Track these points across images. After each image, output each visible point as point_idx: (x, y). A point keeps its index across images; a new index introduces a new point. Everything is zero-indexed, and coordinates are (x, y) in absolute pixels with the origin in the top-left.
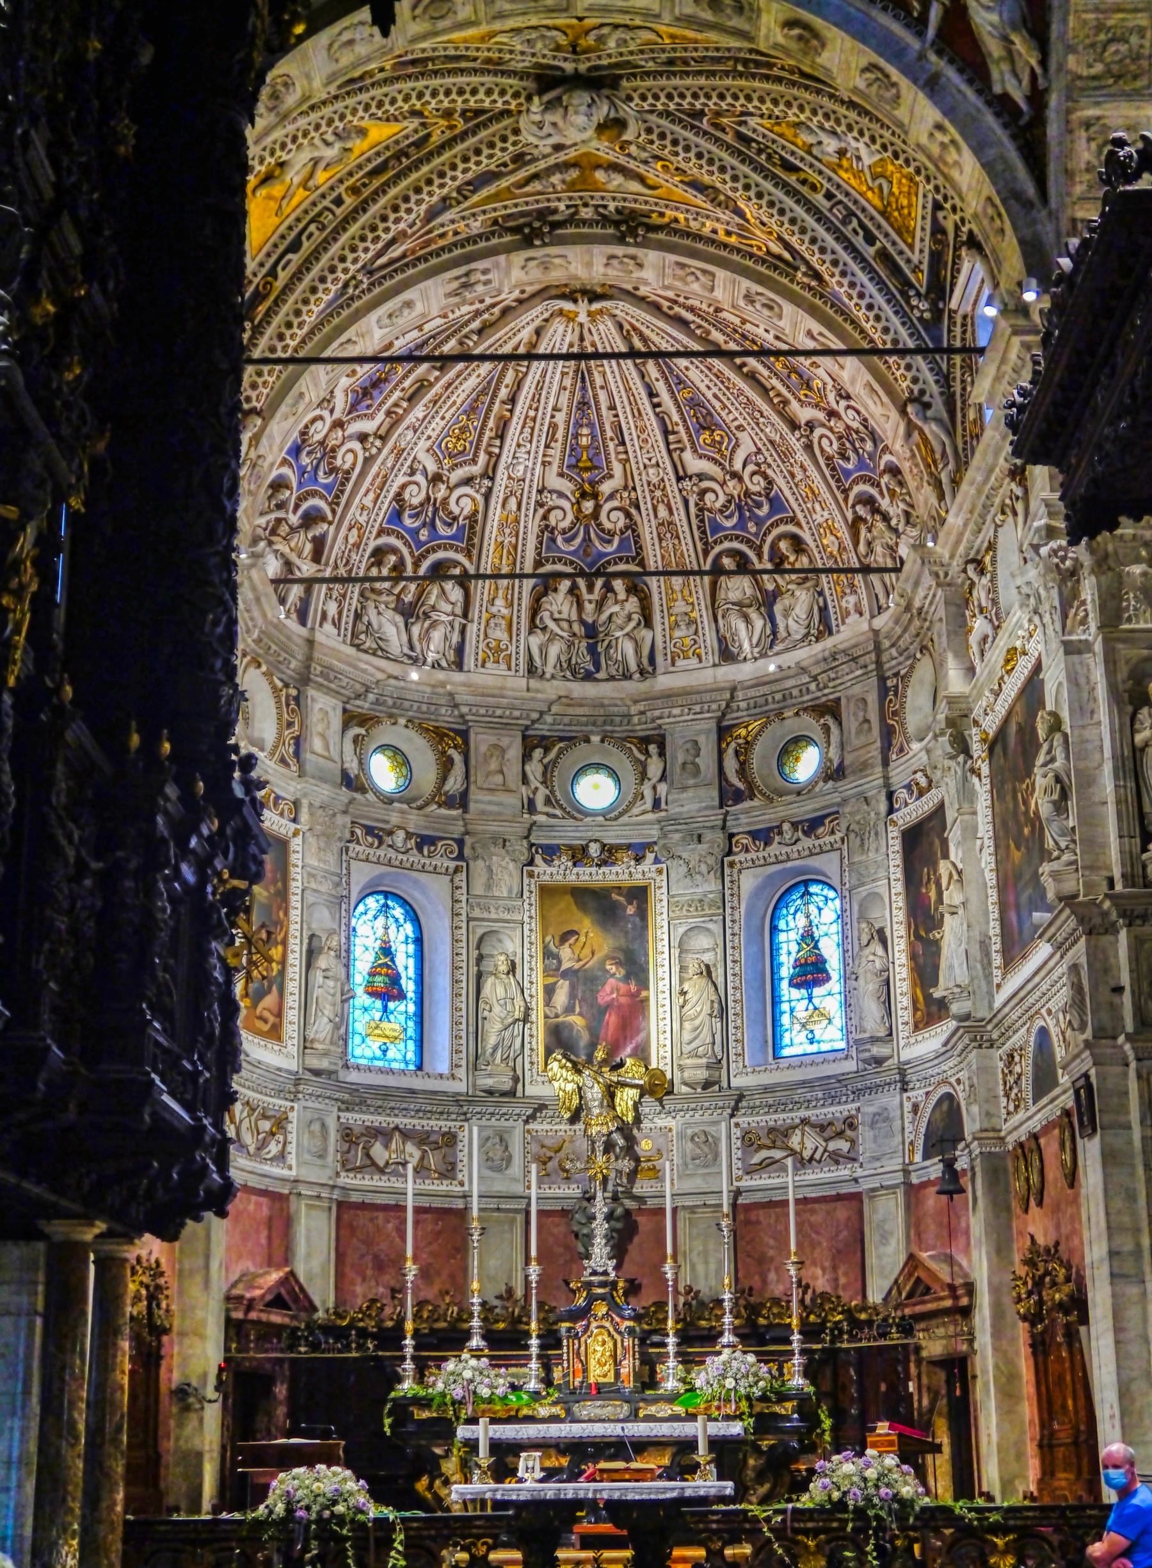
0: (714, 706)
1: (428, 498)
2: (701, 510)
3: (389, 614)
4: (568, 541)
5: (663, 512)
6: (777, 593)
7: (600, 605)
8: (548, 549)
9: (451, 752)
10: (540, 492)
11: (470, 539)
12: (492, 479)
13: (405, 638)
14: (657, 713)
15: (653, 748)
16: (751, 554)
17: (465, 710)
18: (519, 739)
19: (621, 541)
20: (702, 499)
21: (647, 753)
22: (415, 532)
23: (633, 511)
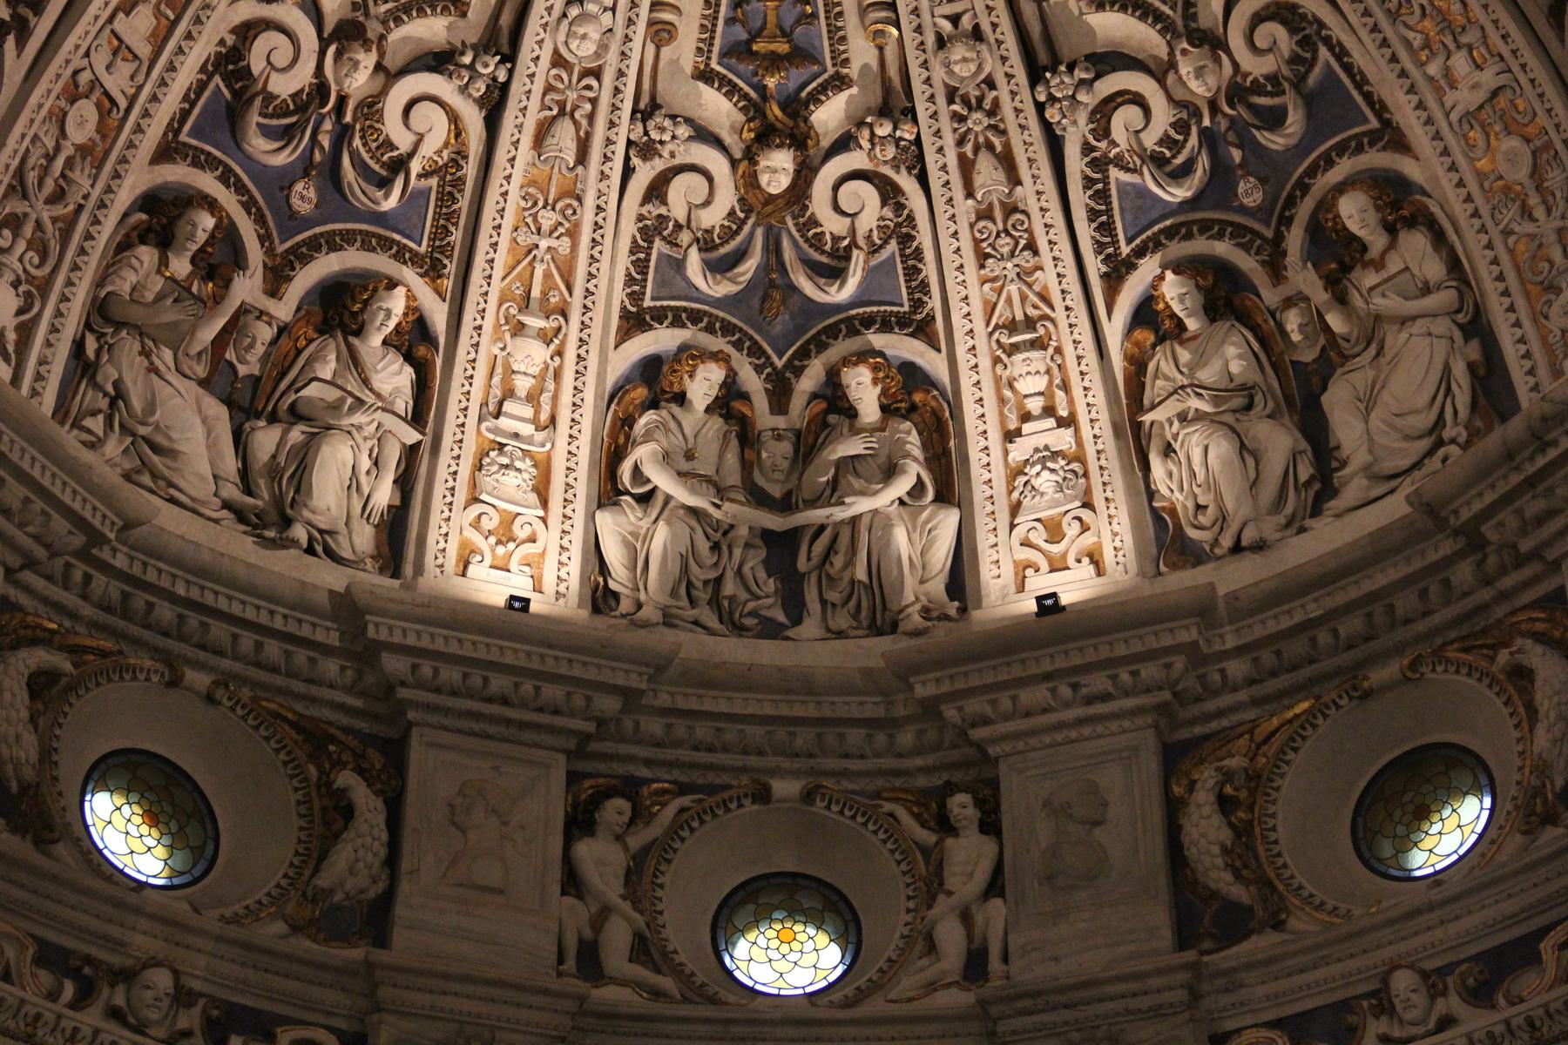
0: (1150, 671)
1: (320, 89)
2: (1099, 164)
3: (189, 388)
4: (721, 267)
5: (988, 174)
6: (1333, 357)
7: (807, 445)
8: (661, 283)
9: (346, 779)
10: (646, 111)
11: (441, 232)
12: (510, 58)
13: (231, 464)
14: (975, 706)
15: (962, 806)
16: (1246, 263)
17: (395, 665)
18: (559, 776)
19: (870, 274)
20: (1104, 132)
21: (945, 825)
22: (280, 183)
23: (907, 182)
